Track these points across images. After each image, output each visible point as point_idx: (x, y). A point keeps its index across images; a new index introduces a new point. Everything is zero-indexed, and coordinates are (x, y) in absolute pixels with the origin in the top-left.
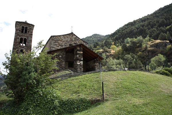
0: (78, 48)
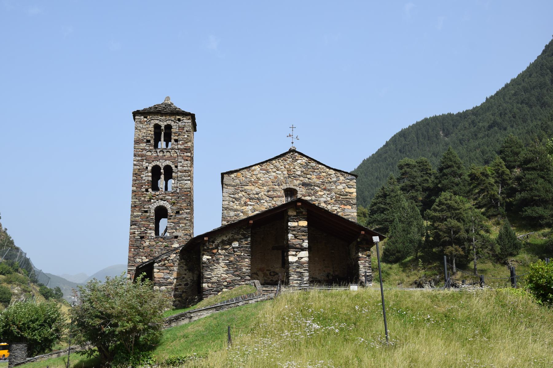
0: (292, 213)
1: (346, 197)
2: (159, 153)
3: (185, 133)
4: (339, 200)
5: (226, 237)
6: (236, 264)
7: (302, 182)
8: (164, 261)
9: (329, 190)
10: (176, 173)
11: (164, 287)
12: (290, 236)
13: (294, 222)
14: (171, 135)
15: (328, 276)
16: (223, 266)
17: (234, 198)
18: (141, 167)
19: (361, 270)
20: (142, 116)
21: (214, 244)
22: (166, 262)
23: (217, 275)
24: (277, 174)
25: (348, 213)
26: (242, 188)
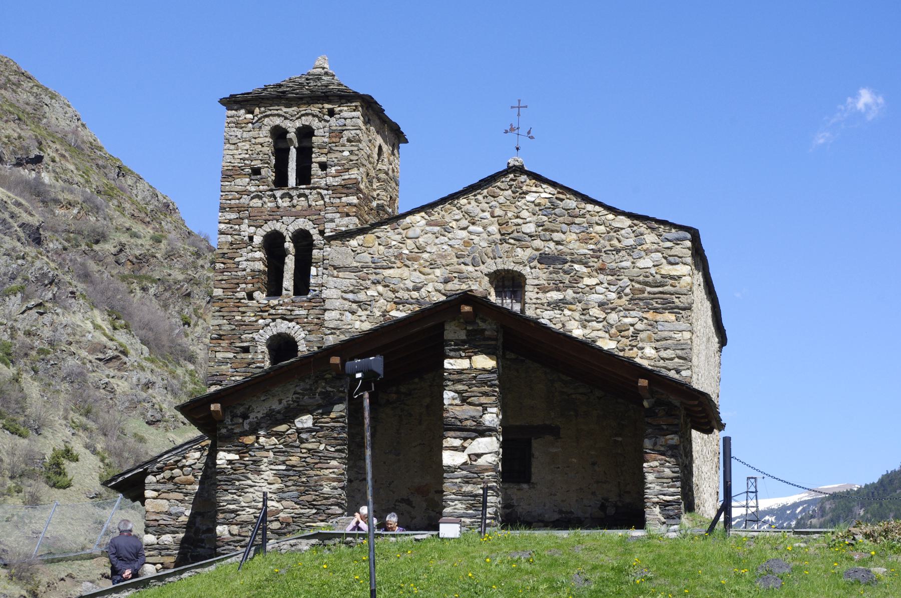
1: (660, 289)
2: (280, 201)
3: (344, 145)
4: (640, 299)
5: (280, 402)
6: (305, 474)
7: (537, 253)
8: (172, 469)
9: (613, 273)
10: (320, 249)
11: (169, 535)
12: (448, 396)
13: (461, 357)
14: (312, 152)
15: (603, 507)
16: (271, 478)
17: (354, 302)
18: (236, 237)
19: (649, 488)
20: (241, 108)
21: (248, 421)
22: (177, 471)
23: (253, 503)
24: (470, 233)
25: (666, 334)
26: (375, 273)
